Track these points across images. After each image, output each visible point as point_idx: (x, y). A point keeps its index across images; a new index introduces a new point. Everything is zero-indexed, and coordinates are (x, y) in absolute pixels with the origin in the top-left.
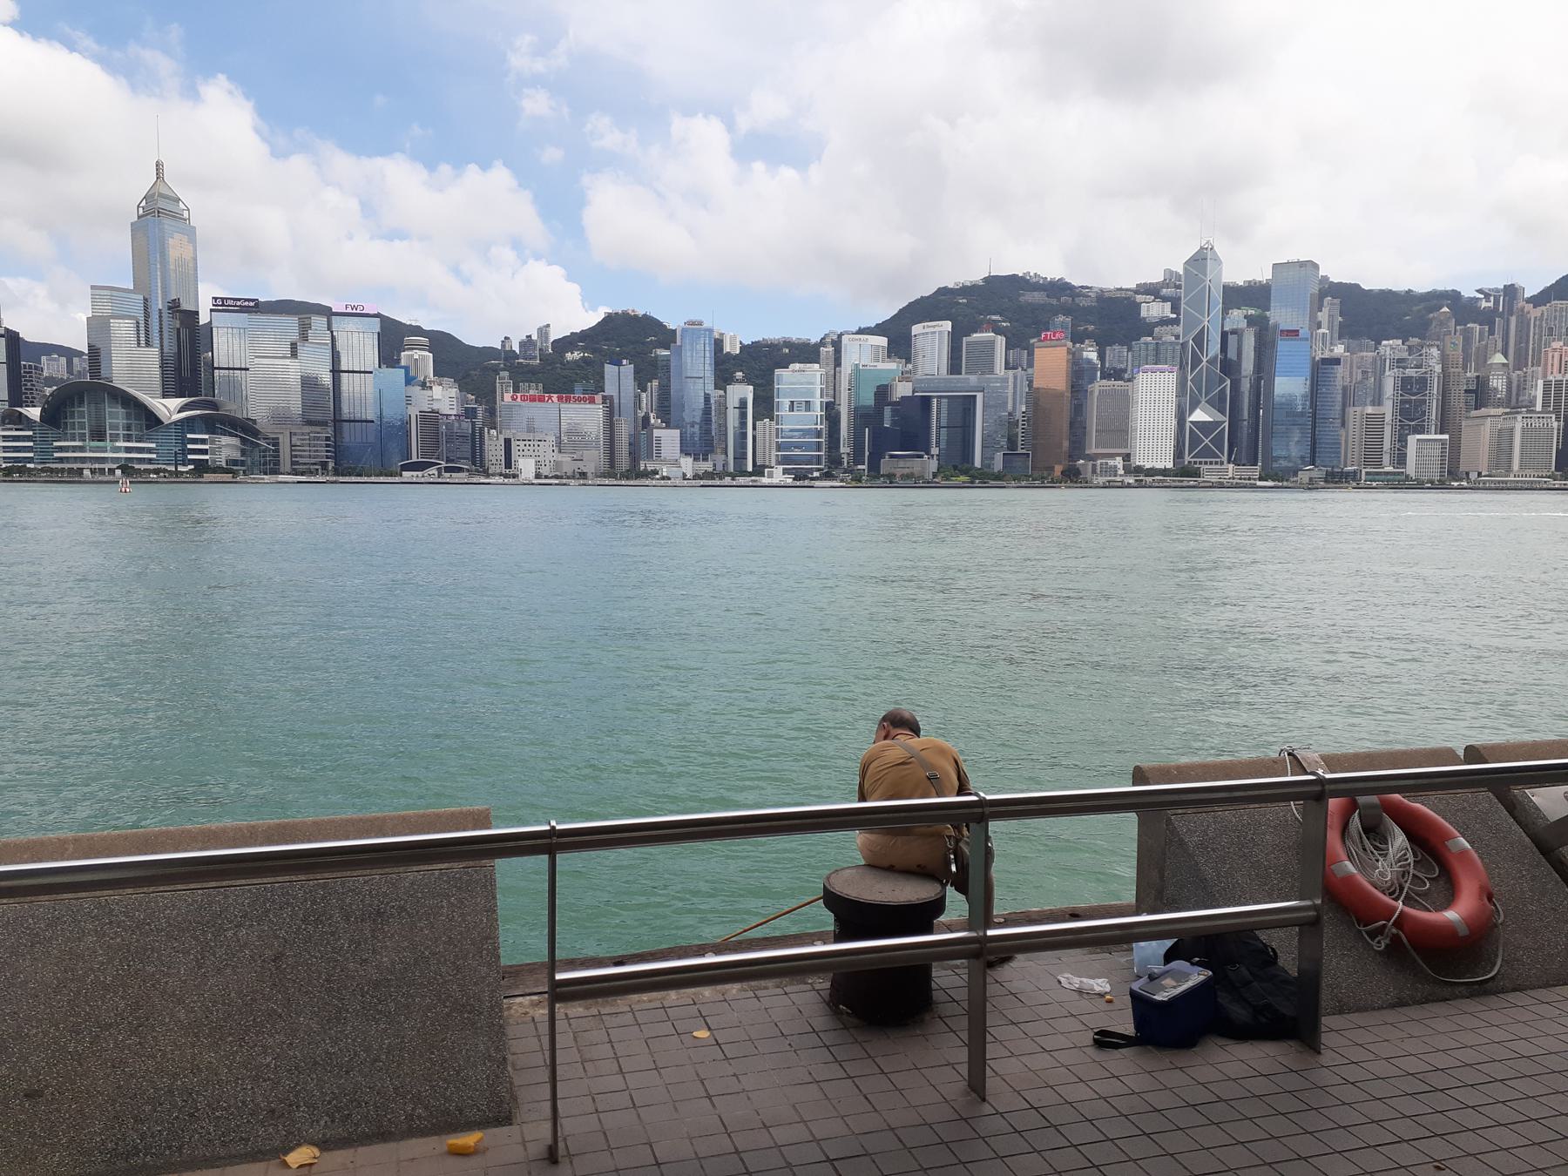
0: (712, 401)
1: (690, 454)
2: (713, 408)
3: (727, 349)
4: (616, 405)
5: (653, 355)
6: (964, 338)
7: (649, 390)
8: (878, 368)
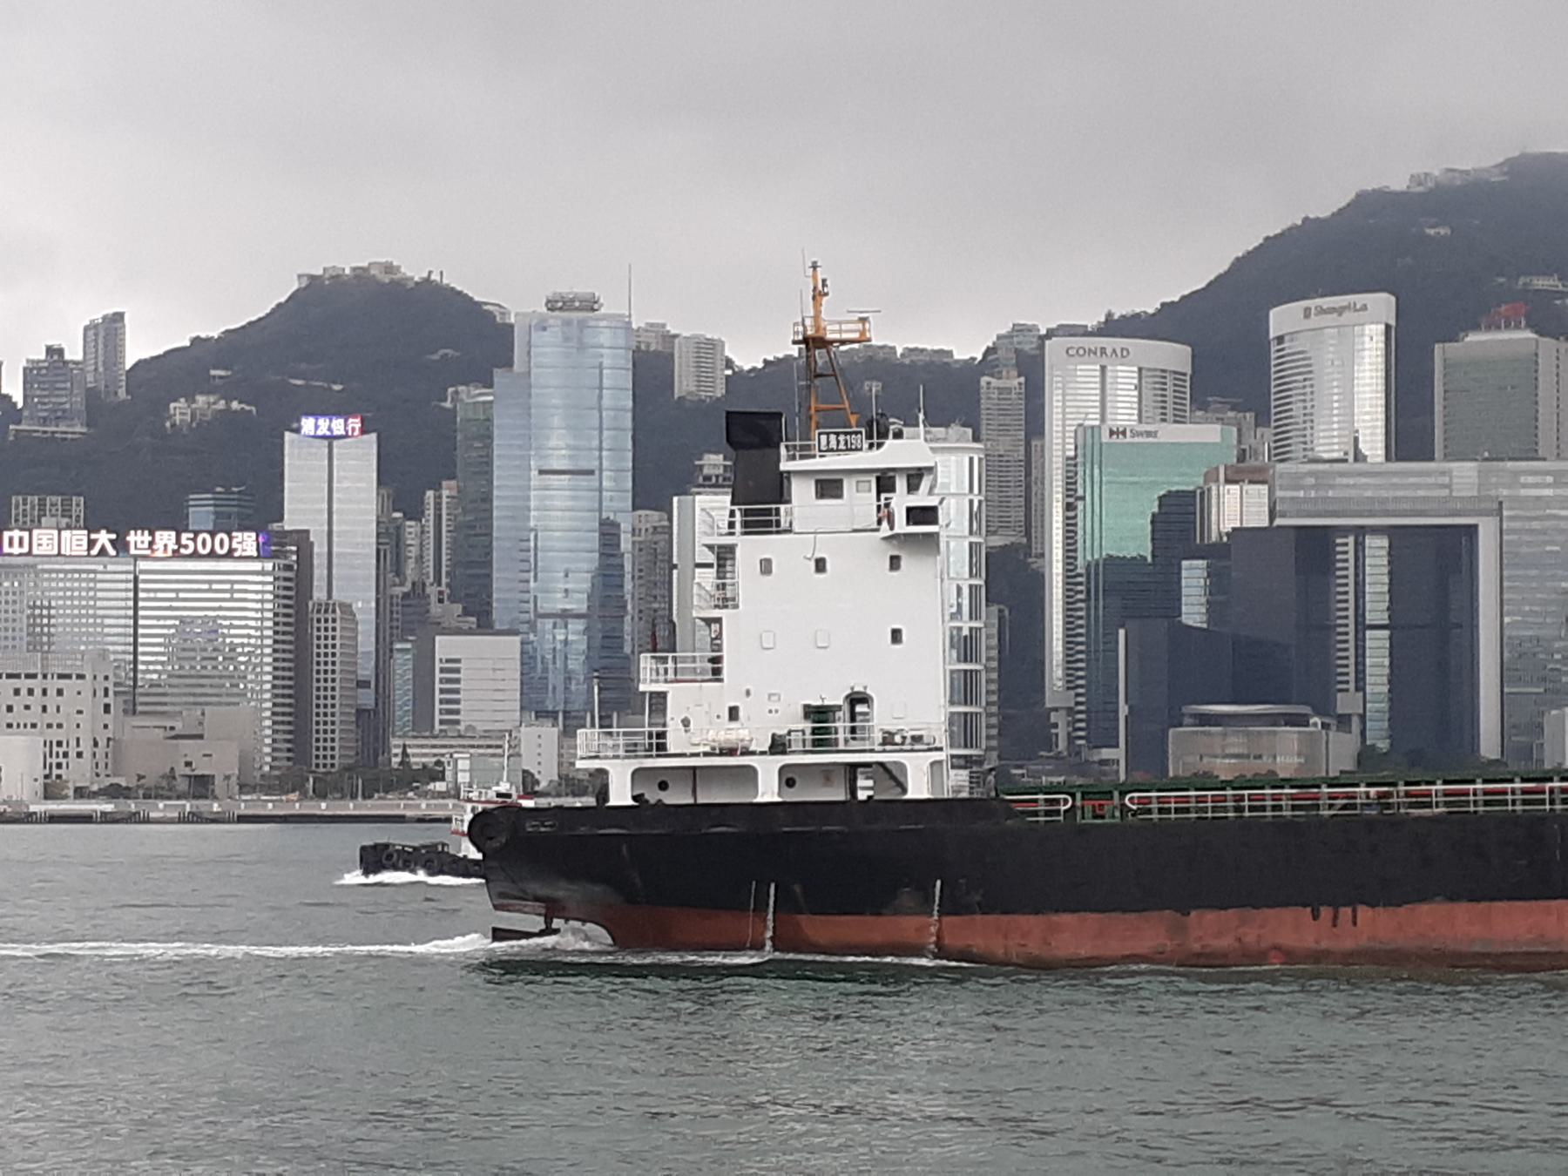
0: (626, 543)
1: (553, 715)
2: (628, 567)
3: (684, 384)
4: (319, 562)
5: (448, 405)
6: (1438, 347)
7: (430, 512)
8: (1162, 438)
